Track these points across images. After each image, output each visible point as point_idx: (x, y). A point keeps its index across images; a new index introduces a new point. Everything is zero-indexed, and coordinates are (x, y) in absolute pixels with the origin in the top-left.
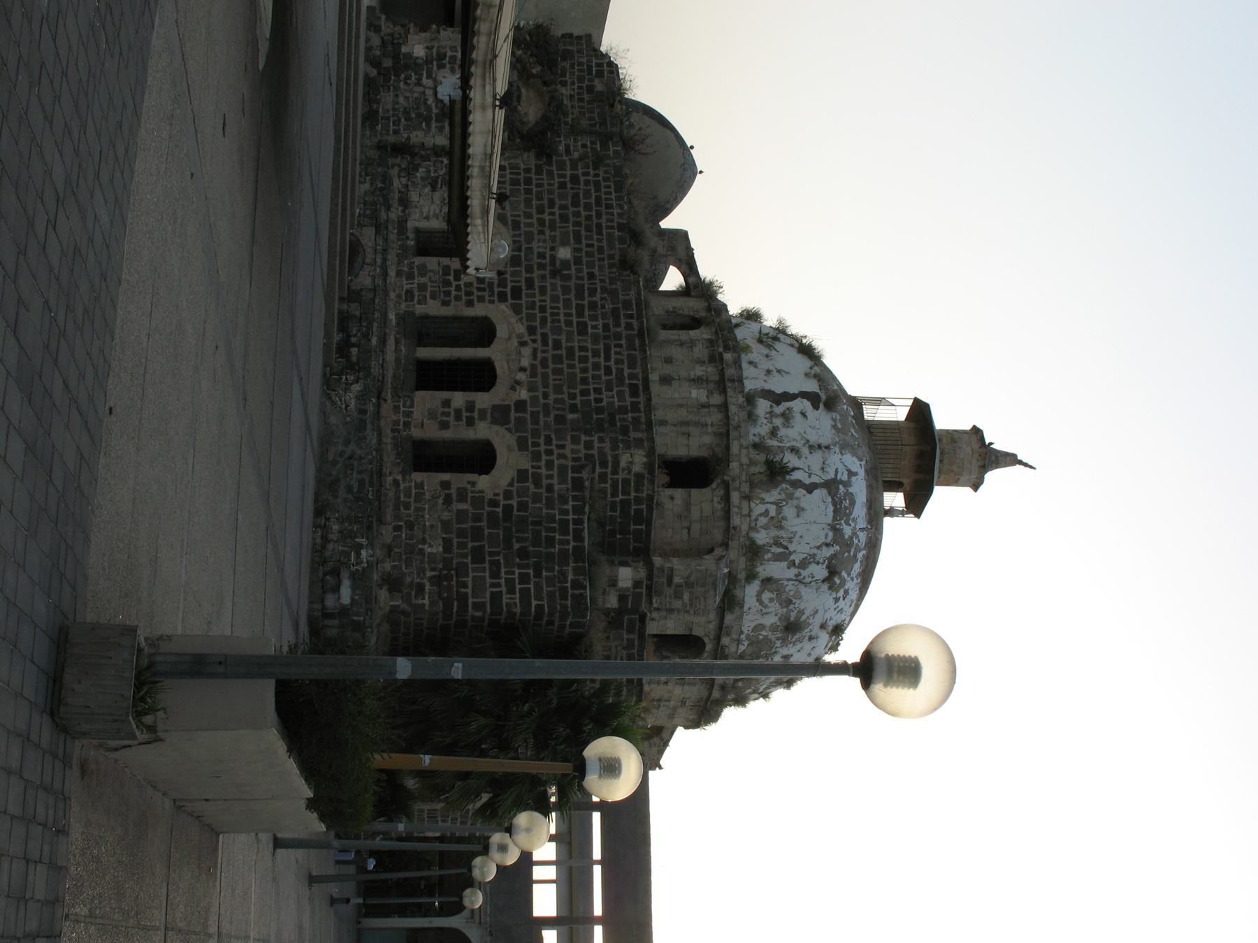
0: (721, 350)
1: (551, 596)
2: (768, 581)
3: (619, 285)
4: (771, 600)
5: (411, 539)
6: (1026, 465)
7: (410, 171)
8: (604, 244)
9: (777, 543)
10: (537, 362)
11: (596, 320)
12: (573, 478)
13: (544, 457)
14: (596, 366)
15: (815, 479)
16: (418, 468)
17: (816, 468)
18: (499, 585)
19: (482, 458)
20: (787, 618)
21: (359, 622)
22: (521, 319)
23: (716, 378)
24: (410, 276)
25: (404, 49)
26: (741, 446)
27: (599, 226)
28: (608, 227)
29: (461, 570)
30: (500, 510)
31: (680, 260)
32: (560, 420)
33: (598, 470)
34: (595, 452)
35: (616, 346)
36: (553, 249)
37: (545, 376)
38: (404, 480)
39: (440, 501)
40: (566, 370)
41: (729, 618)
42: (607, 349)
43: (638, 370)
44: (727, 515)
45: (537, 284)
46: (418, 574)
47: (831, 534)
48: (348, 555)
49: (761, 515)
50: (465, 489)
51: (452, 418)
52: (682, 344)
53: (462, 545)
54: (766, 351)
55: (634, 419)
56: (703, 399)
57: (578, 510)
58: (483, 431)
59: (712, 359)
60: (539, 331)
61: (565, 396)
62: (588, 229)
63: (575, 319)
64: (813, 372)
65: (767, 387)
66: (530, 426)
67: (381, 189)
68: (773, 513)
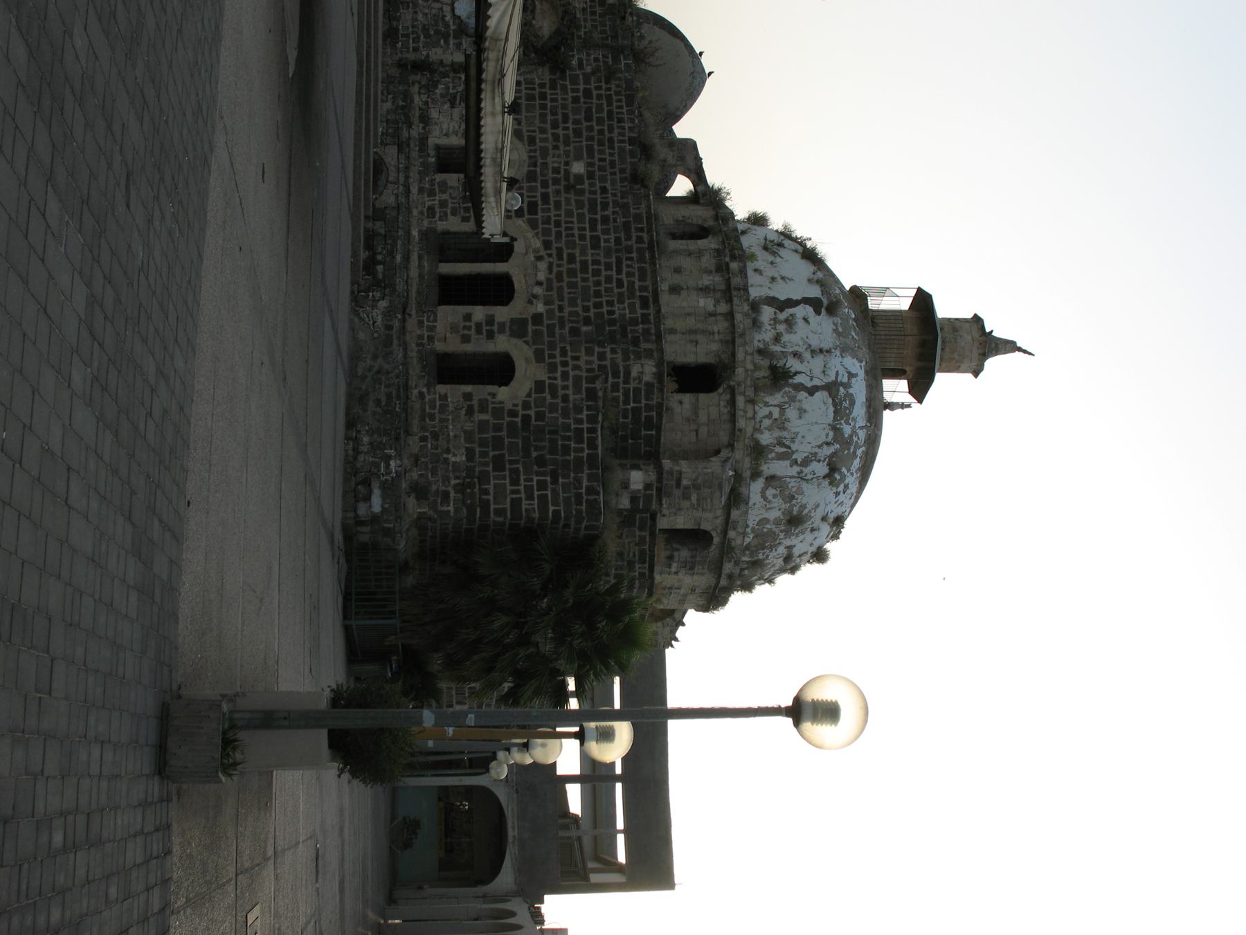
0: (727, 259)
1: (567, 501)
2: (771, 479)
3: (630, 200)
4: (775, 496)
5: (436, 448)
6: (1025, 352)
7: (430, 87)
8: (616, 157)
9: (780, 444)
10: (553, 276)
11: (609, 234)
12: (587, 389)
13: (560, 369)
14: (609, 279)
15: (817, 382)
16: (442, 381)
17: (817, 371)
18: (518, 492)
19: (501, 370)
20: (790, 512)
21: (389, 529)
22: (537, 234)
23: (723, 287)
24: (432, 193)
26: (746, 352)
27: (611, 140)
28: (620, 141)
29: (484, 478)
30: (518, 420)
31: (689, 170)
32: (575, 332)
33: (610, 380)
34: (607, 363)
35: (628, 259)
36: (567, 164)
37: (560, 289)
38: (429, 393)
39: (463, 412)
40: (580, 284)
41: (735, 514)
42: (619, 262)
43: (648, 283)
44: (733, 418)
45: (552, 199)
46: (443, 483)
47: (831, 434)
48: (378, 466)
49: (765, 417)
50: (486, 400)
51: (473, 332)
52: (690, 255)
53: (484, 454)
54: (771, 258)
55: (642, 331)
56: (711, 308)
57: (592, 419)
58: (502, 343)
59: (719, 269)
60: (555, 245)
61: (579, 309)
62: (601, 143)
63: (588, 234)
64: (816, 277)
65: (771, 294)
66: (546, 339)
67: (403, 108)
68: (776, 415)
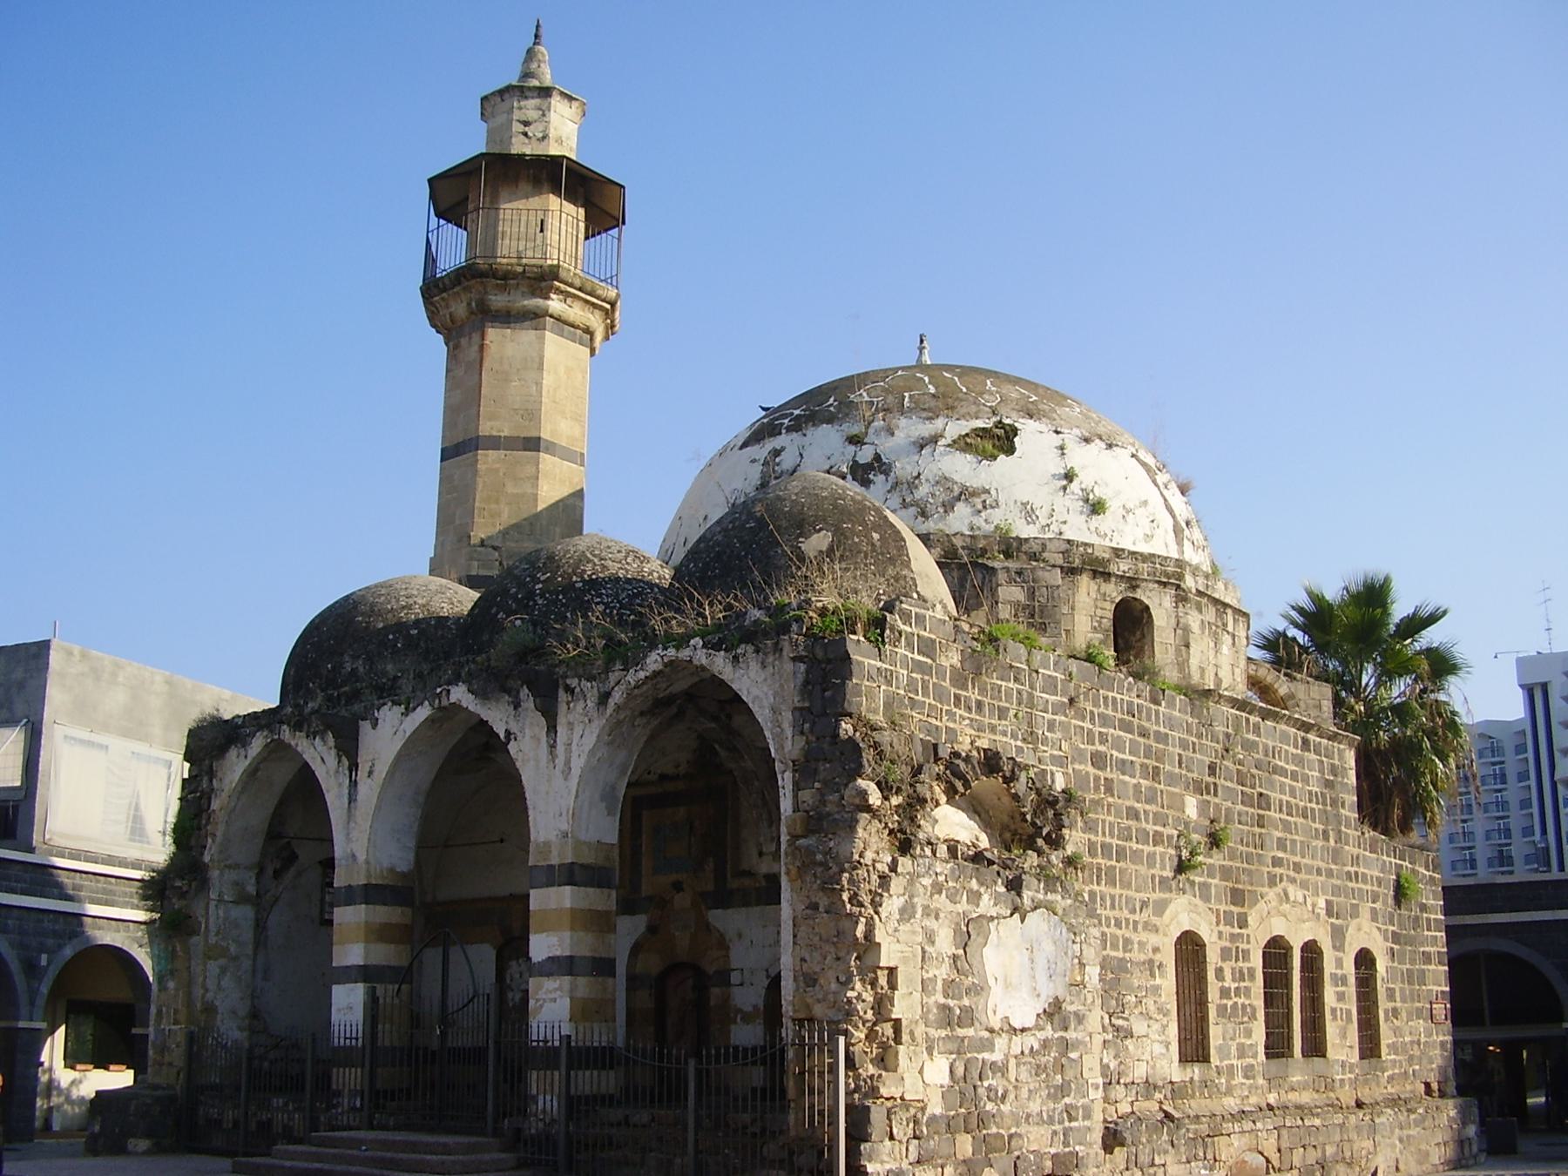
25: (936, 1108)
